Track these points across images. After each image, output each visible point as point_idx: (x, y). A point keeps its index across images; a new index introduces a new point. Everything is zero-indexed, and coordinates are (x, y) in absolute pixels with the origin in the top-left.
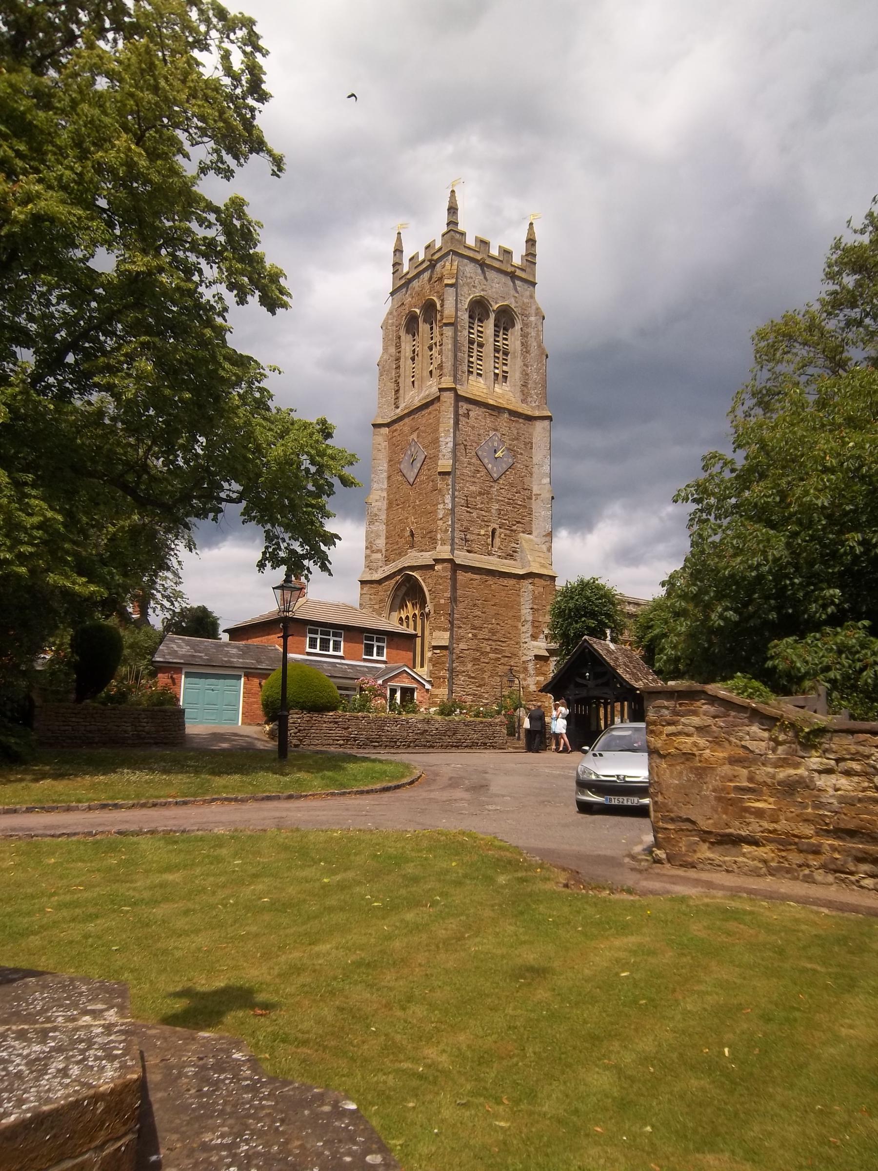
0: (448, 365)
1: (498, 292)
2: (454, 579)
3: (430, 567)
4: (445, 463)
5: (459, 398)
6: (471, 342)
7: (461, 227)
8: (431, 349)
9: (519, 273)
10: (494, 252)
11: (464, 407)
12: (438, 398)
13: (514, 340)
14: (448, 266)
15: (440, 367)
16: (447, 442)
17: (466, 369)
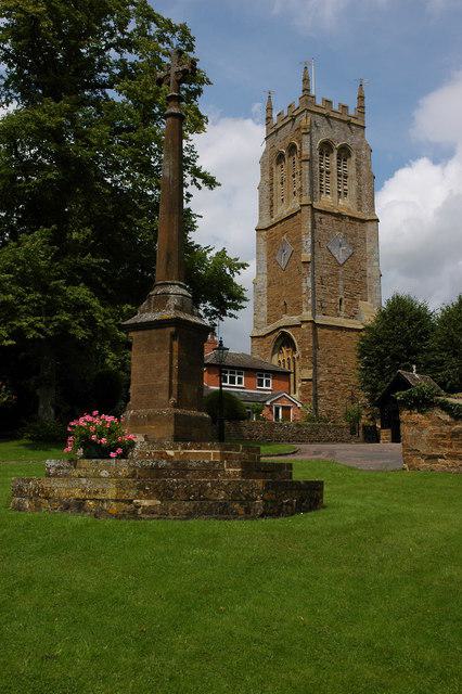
0: (307, 188)
1: (338, 135)
2: (315, 334)
3: (299, 326)
4: (306, 256)
5: (314, 210)
6: (322, 171)
7: (313, 93)
8: (294, 176)
9: (353, 121)
10: (335, 107)
11: (318, 215)
12: (300, 211)
13: (351, 169)
14: (303, 121)
15: (300, 190)
16: (307, 241)
17: (318, 190)
